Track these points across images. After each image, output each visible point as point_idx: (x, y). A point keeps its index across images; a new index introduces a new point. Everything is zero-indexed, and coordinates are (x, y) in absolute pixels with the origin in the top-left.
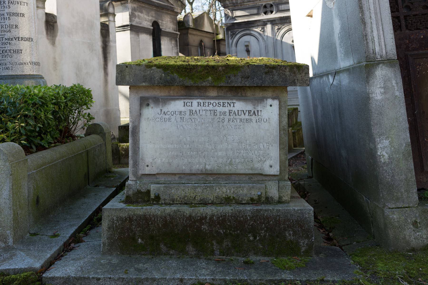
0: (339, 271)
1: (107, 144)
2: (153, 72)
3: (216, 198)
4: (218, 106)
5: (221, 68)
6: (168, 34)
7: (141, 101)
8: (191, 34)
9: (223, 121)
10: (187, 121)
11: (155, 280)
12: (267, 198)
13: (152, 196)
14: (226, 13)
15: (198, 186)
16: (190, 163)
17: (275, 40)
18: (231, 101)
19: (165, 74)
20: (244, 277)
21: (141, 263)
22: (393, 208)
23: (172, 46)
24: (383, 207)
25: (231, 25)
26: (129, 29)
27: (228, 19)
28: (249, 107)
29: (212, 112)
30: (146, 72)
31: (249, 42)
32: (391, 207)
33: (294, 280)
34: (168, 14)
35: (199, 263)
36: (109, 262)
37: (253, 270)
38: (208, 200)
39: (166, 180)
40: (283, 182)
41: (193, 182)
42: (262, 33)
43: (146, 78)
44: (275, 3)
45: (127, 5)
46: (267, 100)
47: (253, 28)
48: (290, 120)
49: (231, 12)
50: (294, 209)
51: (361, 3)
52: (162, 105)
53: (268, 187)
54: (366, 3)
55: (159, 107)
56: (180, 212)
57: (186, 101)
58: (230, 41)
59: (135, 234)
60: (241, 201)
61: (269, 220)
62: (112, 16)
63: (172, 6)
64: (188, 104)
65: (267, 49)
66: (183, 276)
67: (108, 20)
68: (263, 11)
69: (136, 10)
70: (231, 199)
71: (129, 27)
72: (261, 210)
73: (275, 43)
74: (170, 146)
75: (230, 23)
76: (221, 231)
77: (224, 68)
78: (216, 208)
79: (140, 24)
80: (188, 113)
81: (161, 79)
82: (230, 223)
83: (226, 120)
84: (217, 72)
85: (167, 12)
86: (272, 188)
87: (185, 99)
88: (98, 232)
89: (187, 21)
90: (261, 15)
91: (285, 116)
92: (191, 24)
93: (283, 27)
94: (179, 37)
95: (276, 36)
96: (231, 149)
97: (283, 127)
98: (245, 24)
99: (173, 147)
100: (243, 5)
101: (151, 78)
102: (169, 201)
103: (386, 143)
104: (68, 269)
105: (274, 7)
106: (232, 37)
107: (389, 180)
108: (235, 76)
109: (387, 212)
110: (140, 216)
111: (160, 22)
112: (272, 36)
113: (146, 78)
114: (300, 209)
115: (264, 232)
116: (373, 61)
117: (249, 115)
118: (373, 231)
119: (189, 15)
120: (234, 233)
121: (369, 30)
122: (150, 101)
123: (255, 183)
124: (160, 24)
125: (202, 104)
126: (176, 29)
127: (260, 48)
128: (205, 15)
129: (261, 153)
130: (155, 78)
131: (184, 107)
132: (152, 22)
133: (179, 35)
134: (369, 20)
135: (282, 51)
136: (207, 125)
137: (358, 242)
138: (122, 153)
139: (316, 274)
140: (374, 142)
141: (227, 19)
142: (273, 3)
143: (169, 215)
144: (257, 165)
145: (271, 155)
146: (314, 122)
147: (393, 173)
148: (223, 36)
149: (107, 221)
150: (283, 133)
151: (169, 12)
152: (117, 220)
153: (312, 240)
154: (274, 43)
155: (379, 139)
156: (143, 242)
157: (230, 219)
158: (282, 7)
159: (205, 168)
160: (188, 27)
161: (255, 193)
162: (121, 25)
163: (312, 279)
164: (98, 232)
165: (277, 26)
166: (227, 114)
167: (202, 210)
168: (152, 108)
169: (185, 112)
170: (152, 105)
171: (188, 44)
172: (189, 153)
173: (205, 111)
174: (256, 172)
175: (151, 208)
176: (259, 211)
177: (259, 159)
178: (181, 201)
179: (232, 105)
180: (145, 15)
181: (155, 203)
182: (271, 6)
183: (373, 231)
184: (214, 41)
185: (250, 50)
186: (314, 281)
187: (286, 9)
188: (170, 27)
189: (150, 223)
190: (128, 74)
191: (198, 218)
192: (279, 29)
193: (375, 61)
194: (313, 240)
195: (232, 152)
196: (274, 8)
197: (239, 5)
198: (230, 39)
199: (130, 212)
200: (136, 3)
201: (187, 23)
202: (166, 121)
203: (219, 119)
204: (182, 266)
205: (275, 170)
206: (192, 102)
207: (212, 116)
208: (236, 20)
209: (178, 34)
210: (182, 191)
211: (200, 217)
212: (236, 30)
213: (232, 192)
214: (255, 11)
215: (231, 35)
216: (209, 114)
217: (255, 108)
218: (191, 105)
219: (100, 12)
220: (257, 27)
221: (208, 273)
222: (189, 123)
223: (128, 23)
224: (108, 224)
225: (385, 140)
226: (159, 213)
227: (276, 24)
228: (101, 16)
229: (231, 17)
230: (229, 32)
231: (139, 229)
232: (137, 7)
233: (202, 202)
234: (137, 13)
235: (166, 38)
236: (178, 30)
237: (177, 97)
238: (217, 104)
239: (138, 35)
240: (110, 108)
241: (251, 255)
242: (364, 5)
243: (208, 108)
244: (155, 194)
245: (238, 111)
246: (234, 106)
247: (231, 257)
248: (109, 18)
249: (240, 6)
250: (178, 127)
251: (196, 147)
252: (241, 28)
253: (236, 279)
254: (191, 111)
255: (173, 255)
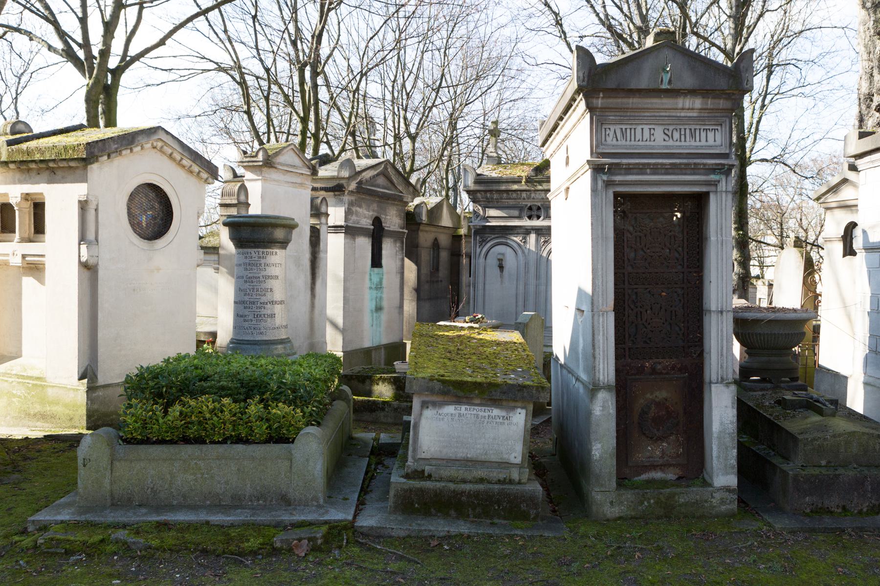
6: (394, 235)
8: (422, 231)
31: (503, 254)
34: (394, 204)
58: (478, 250)
92: (424, 218)
124: (383, 220)
162: (332, 225)
182: (539, 208)
198: (478, 247)
208: (489, 222)
209: (405, 233)
212: (487, 235)
214: (516, 213)
223: (342, 223)
230: (478, 238)
234: (354, 209)
252: (494, 234)
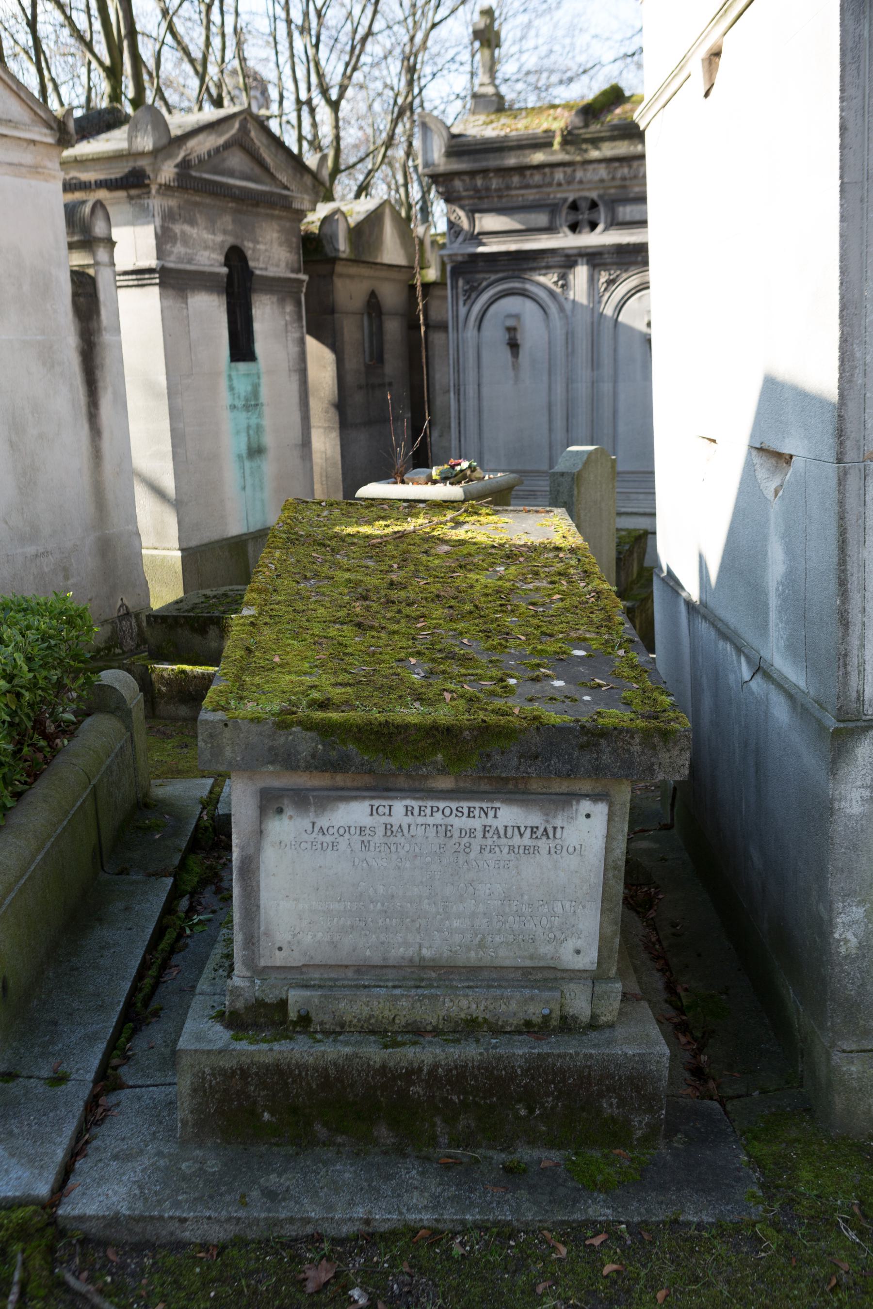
0: (714, 1194)
1: (136, 739)
2: (293, 740)
3: (444, 1019)
4: (456, 816)
5: (467, 733)
6: (275, 285)
7: (261, 801)
8: (341, 276)
9: (467, 850)
10: (378, 850)
11: (309, 1222)
12: (563, 1018)
13: (293, 1015)
14: (452, 218)
15: (403, 995)
16: (383, 943)
17: (596, 315)
18: (490, 805)
19: (324, 745)
20: (505, 1215)
21: (274, 1170)
22: (851, 1052)
23: (286, 321)
24: (830, 1047)
25: (466, 258)
26: (157, 281)
27: (457, 237)
28: (535, 818)
29: (442, 830)
30: (275, 740)
31: (517, 317)
32: (848, 1049)
33: (613, 1221)
34: (272, 217)
35: (403, 1172)
36: (201, 1169)
37: (523, 1194)
38: (425, 1024)
39: (326, 976)
40: (603, 985)
41: (390, 984)
42: (558, 290)
43: (276, 755)
44: (606, 198)
45: (146, 201)
46: (578, 802)
47: (532, 273)
48: (622, 573)
49: (468, 217)
50: (626, 1054)
51: (844, 571)
52: (315, 812)
53: (568, 995)
54: (859, 571)
55: (309, 816)
56: (361, 1058)
57: (376, 803)
58: (463, 311)
59: (255, 1103)
60: (502, 1027)
61: (565, 1076)
62: (105, 247)
63: (286, 192)
64: (381, 809)
65: (570, 341)
66: (370, 1212)
67: (92, 262)
68: (566, 221)
69: (177, 217)
70: (478, 1023)
71: (157, 275)
72: (548, 1054)
73: (595, 325)
74: (335, 906)
75: (463, 255)
76: (455, 1098)
77: (475, 733)
78: (443, 1051)
79: (190, 262)
80: (380, 831)
81: (313, 756)
82: (475, 1082)
83: (476, 848)
84: (457, 744)
85: (268, 211)
86: (577, 997)
87: (373, 798)
88: (153, 1048)
89: (331, 238)
90: (559, 233)
91: (620, 837)
92: (343, 246)
93: (625, 276)
94: (307, 288)
95: (600, 302)
96: (485, 914)
97: (613, 861)
98: (508, 260)
99: (342, 908)
100: (507, 196)
101: (289, 755)
102: (332, 1027)
103: (858, 912)
104: (110, 1192)
105: (602, 209)
106: (469, 297)
107: (852, 993)
108: (502, 753)
109: (837, 1058)
110: (267, 1067)
111: (249, 248)
112: (589, 302)
113: (276, 755)
114: (639, 1054)
115: (553, 1101)
116: (855, 718)
117: (531, 837)
118: (800, 1069)
119: (336, 217)
120: (485, 1103)
121: (855, 642)
122: (286, 801)
123: (538, 988)
124: (249, 254)
125: (416, 812)
126: (296, 266)
127: (549, 337)
128: (387, 212)
129: (556, 923)
130: (300, 754)
131: (370, 818)
132: (226, 250)
133: (305, 284)
134: (860, 615)
135: (615, 350)
136: (429, 859)
137: (764, 1092)
138: (159, 690)
139: (662, 1203)
140: (830, 910)
141: (453, 239)
142: (600, 197)
143: (335, 1064)
144: (545, 949)
145: (581, 926)
146: (689, 685)
147: (863, 978)
148: (439, 273)
149: (189, 1075)
150: (613, 876)
151: (277, 212)
152: (213, 1075)
153: (659, 1116)
154: (592, 323)
155: (841, 905)
156: (274, 1120)
157: (476, 1072)
158: (626, 212)
159: (419, 953)
160: (333, 255)
161: (536, 1011)
162: (130, 268)
163: (653, 1219)
164: (153, 1048)
165: (607, 273)
166: (479, 834)
167: (411, 1055)
168: (291, 817)
169: (373, 829)
170: (289, 811)
171: (332, 310)
172: (380, 921)
173: (423, 827)
174: (541, 964)
175: (292, 1049)
176: (544, 1058)
177: (551, 936)
178: (362, 1027)
179: (491, 813)
180: (204, 232)
181: (298, 1029)
182: (594, 205)
183: (800, 1069)
184: (413, 287)
185: (519, 342)
186: (658, 1223)
187: (637, 218)
188: (280, 260)
189: (290, 1080)
190: (230, 742)
191: (402, 1070)
192: (610, 282)
193: (858, 720)
194: (662, 1117)
195: (486, 920)
196: (599, 213)
197: (495, 194)
198: (461, 303)
199: (243, 1058)
200: (176, 194)
201: (332, 243)
202: (325, 848)
203: (457, 845)
204: (366, 1180)
205: (589, 959)
206: (390, 806)
207: (442, 840)
208: (484, 244)
209: (304, 281)
210: (364, 1006)
211: (407, 1068)
212: (481, 276)
213: (482, 1008)
214: (542, 219)
215: (466, 291)
216: (434, 834)
217: (547, 821)
218: (387, 813)
219: (68, 233)
220: (543, 272)
221: (425, 1202)
222: (383, 854)
223: (151, 262)
224: (192, 1083)
225: (857, 906)
226: (311, 1060)
227: (604, 266)
228: (71, 246)
229: (467, 232)
230: (461, 282)
231: (265, 1092)
232: (179, 207)
233: (410, 1028)
234: (177, 228)
235: (268, 297)
236: (304, 262)
237: (354, 793)
238: (454, 812)
239: (183, 298)
240: (111, 531)
241: (520, 1144)
242: (852, 575)
243: (430, 820)
244: (299, 1011)
245: (506, 827)
246: (495, 817)
247: (474, 1152)
248: (94, 256)
249: (496, 200)
250: (356, 864)
251: (399, 908)
252: (497, 272)
253: (488, 1220)
254: (389, 827)
255: (344, 1145)
